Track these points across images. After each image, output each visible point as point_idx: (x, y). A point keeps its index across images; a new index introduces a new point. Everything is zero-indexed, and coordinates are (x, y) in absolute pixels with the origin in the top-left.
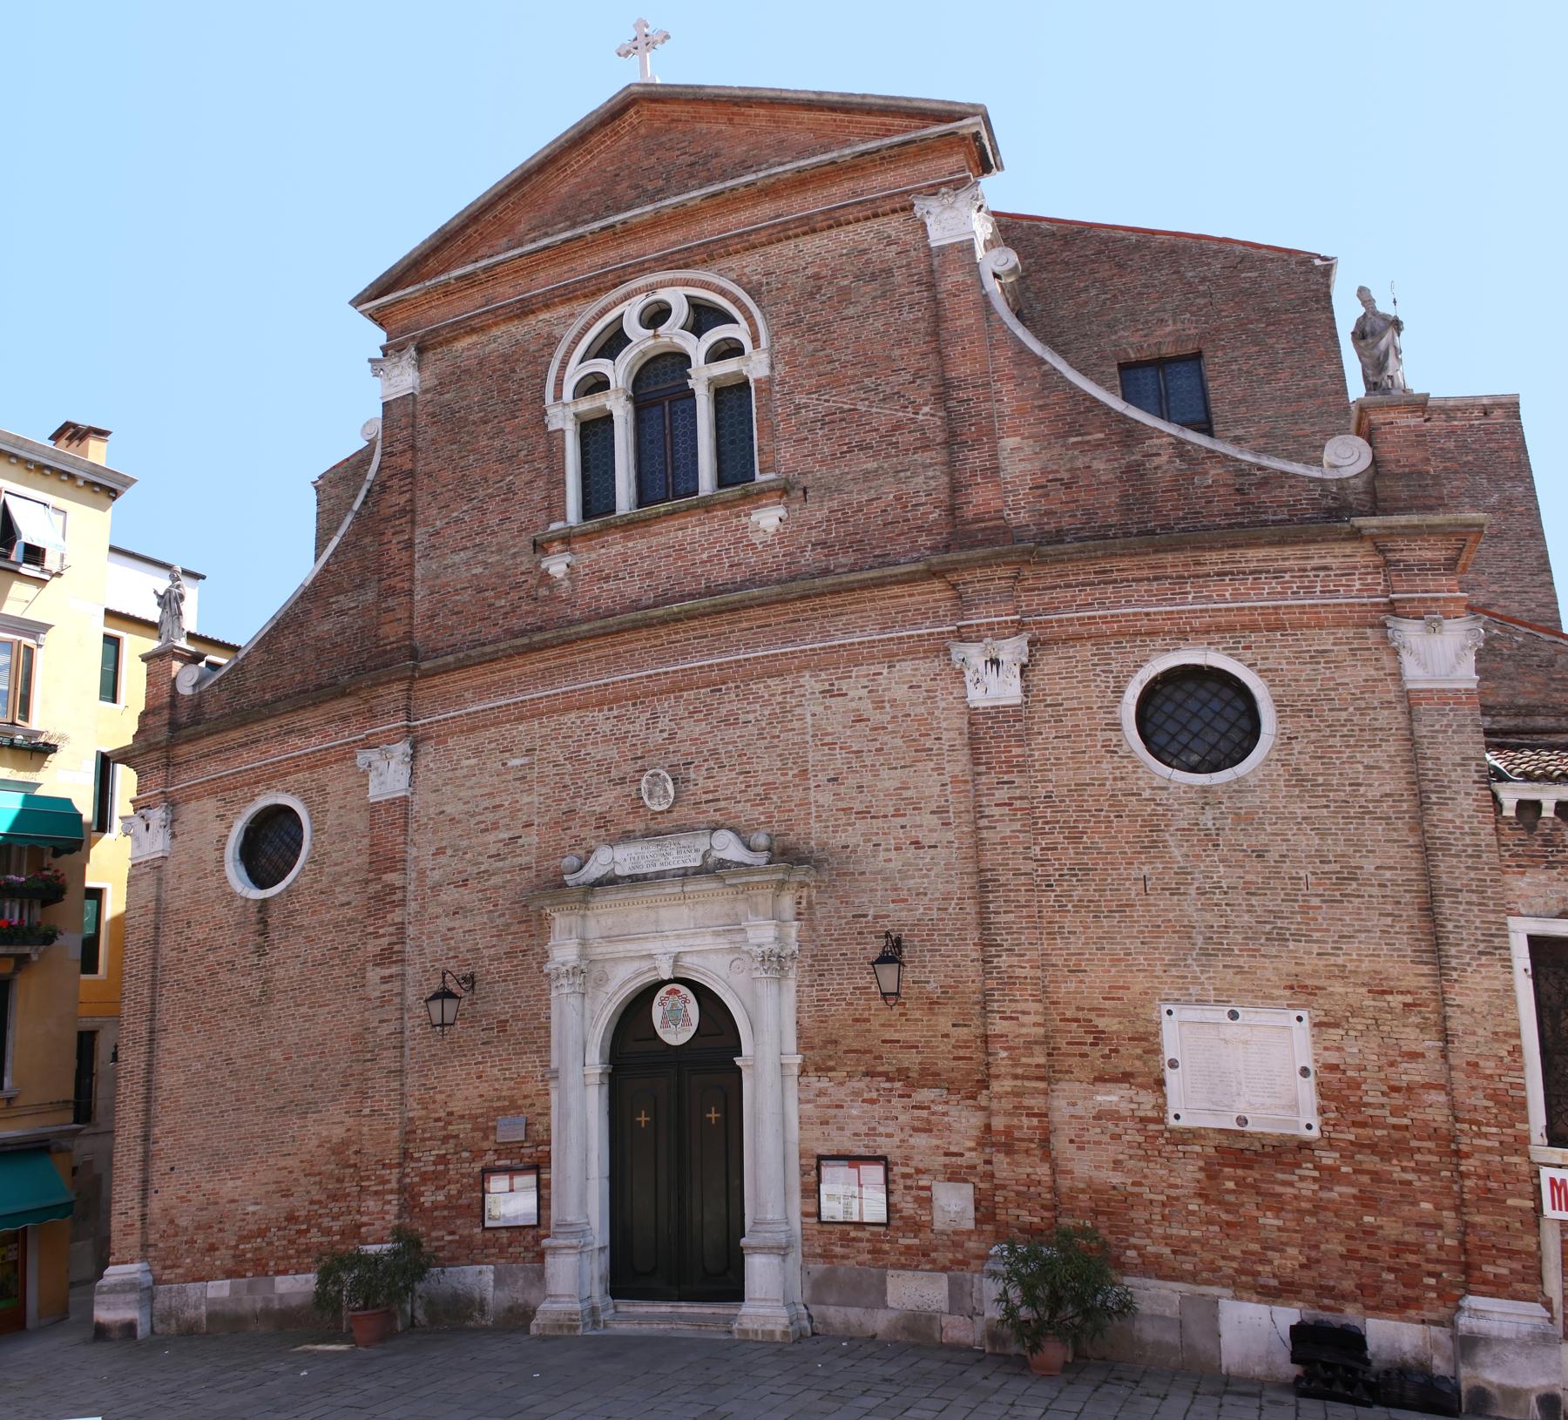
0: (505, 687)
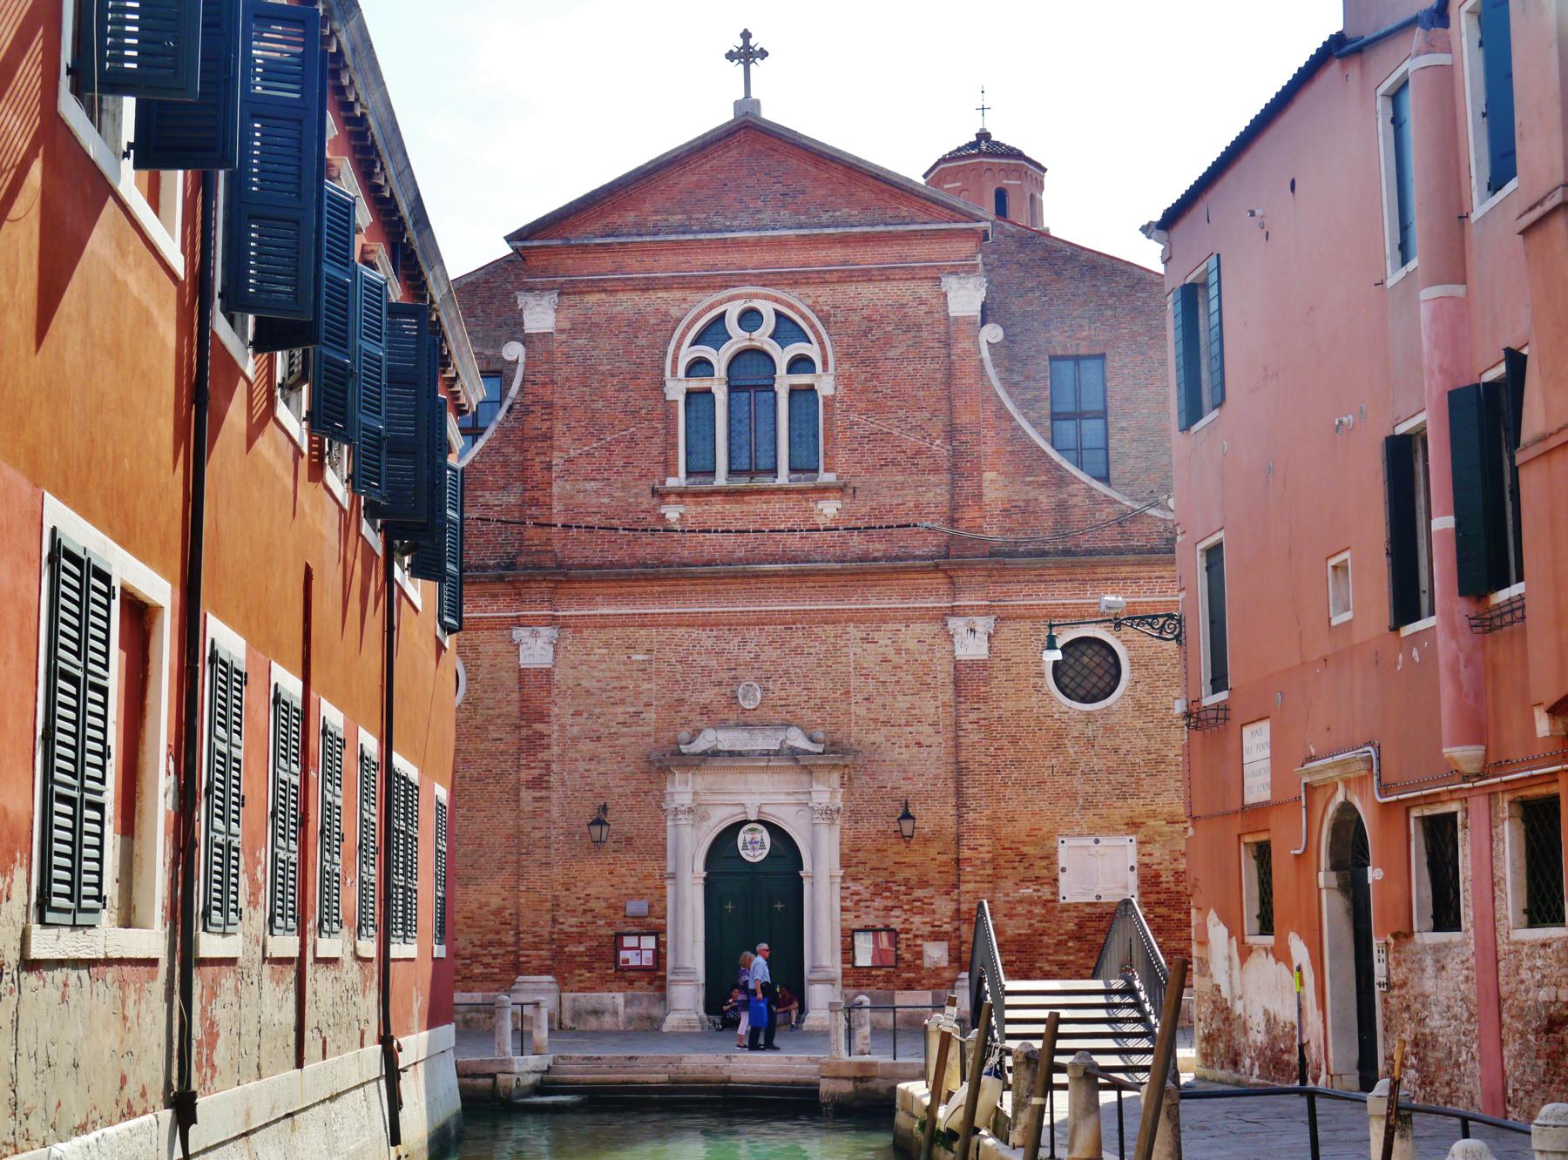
0: (628, 598)
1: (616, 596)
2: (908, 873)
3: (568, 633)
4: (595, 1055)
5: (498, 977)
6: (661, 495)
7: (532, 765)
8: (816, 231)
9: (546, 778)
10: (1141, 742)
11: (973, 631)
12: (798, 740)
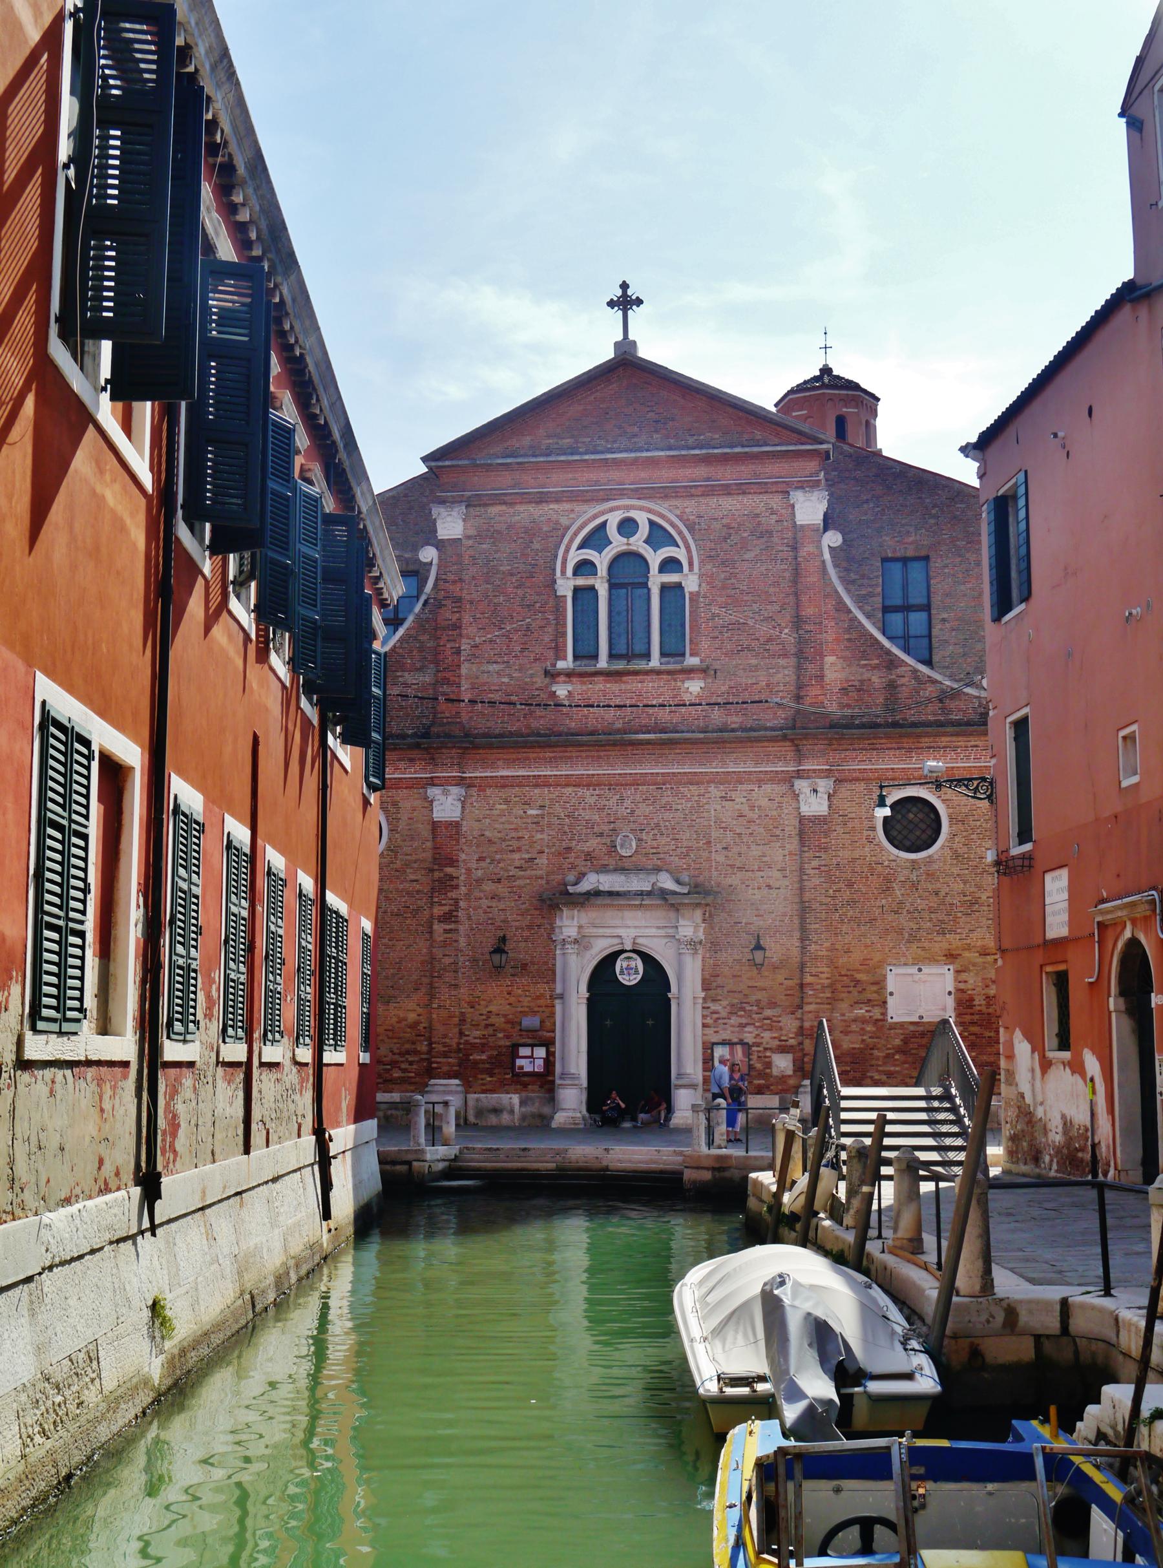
0: (524, 762)
1: (514, 761)
2: (759, 995)
3: (474, 791)
4: (495, 1147)
5: (413, 1080)
6: (552, 675)
7: (443, 902)
8: (683, 452)
9: (455, 913)
10: (959, 886)
11: (815, 791)
12: (666, 882)
